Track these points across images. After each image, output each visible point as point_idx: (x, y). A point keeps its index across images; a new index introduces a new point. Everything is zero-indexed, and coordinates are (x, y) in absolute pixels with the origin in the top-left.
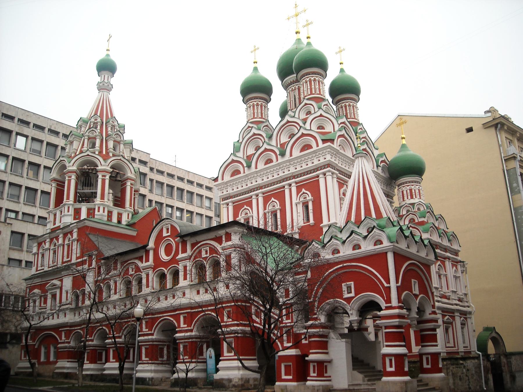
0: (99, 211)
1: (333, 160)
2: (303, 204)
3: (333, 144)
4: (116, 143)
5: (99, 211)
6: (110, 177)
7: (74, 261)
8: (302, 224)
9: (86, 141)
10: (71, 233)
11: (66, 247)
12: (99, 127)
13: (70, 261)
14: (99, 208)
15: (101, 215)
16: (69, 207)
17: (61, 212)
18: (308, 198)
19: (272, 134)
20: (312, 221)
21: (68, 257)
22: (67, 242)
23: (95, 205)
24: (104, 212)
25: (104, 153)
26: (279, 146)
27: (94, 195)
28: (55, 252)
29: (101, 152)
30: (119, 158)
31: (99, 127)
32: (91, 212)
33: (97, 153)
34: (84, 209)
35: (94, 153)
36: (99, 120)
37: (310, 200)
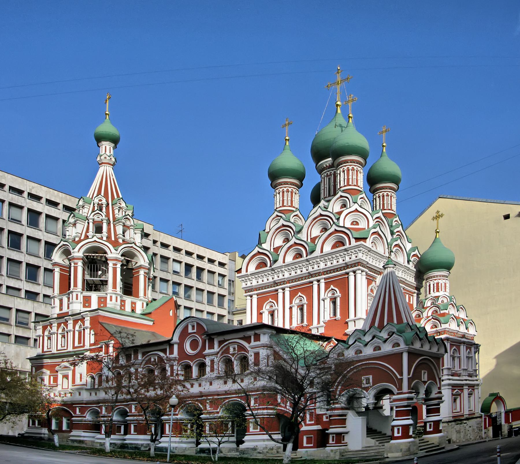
0: (111, 300)
1: (364, 258)
2: (331, 299)
3: (365, 242)
4: (125, 228)
5: (111, 300)
6: (122, 265)
7: (87, 346)
8: (327, 318)
9: (91, 224)
10: (83, 319)
11: (77, 334)
12: (104, 210)
13: (84, 346)
14: (111, 297)
15: (113, 304)
16: (77, 295)
17: (69, 298)
18: (336, 295)
19: (303, 227)
20: (338, 316)
21: (80, 342)
22: (77, 328)
23: (106, 294)
24: (117, 301)
25: (113, 239)
26: (309, 240)
27: (105, 283)
28: (63, 336)
29: (109, 238)
30: (130, 245)
31: (104, 210)
32: (102, 300)
33: (105, 238)
34: (94, 296)
35: (101, 238)
36: (104, 201)
37: (338, 296)
